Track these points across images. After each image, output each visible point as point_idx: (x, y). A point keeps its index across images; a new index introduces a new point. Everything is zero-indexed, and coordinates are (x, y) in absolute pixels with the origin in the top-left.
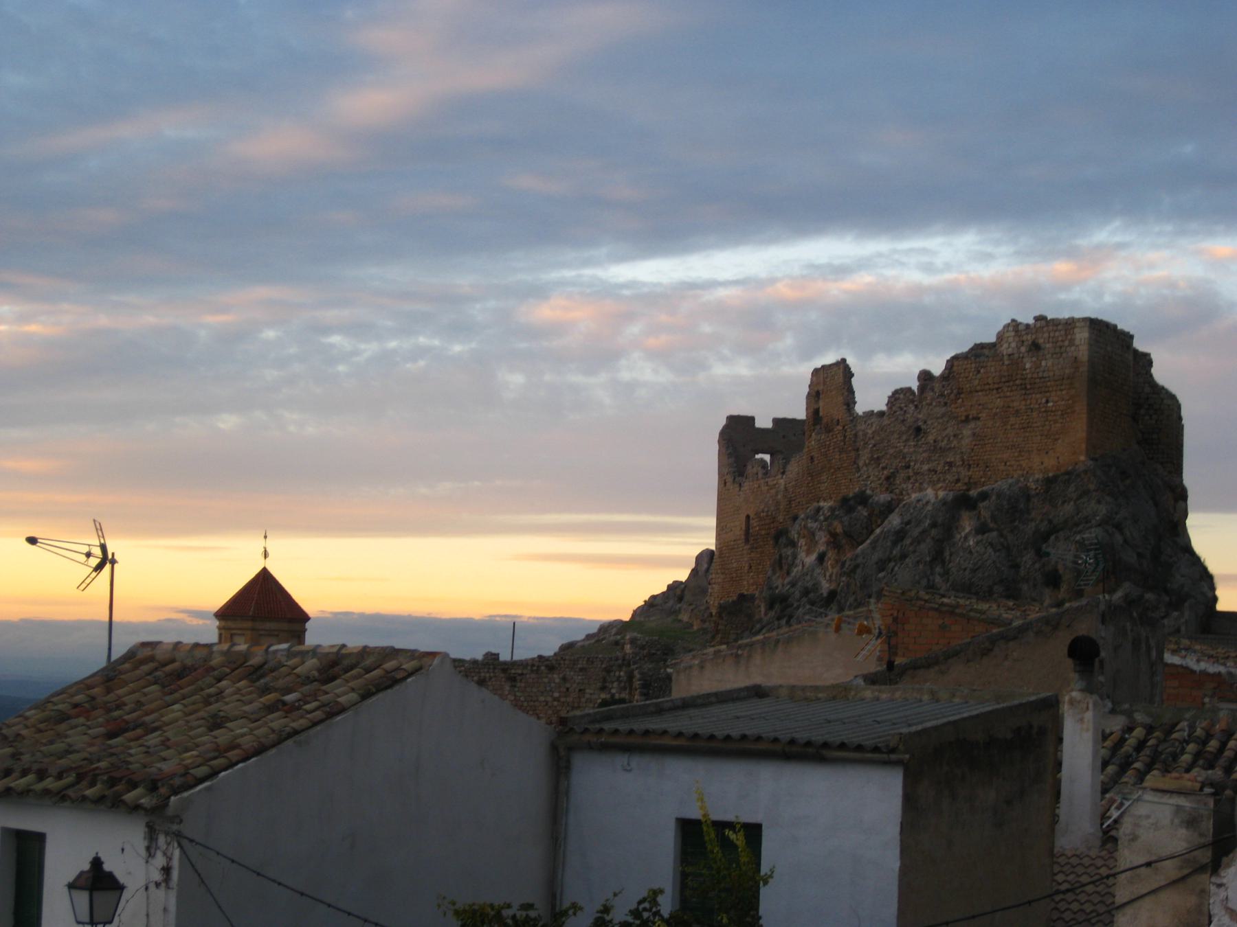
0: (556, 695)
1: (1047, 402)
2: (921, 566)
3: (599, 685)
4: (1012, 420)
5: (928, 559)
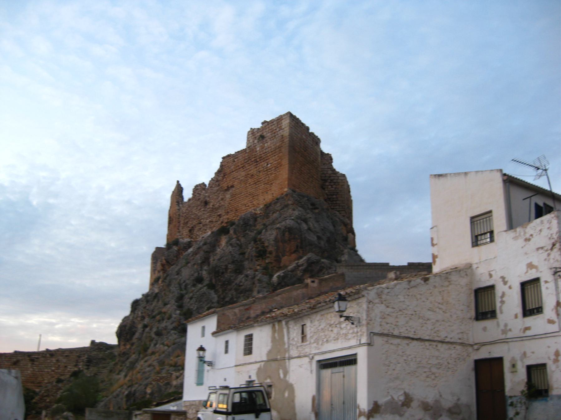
0: (53, 368)
1: (268, 164)
2: (195, 267)
3: (75, 364)
4: (250, 180)
5: (199, 262)
